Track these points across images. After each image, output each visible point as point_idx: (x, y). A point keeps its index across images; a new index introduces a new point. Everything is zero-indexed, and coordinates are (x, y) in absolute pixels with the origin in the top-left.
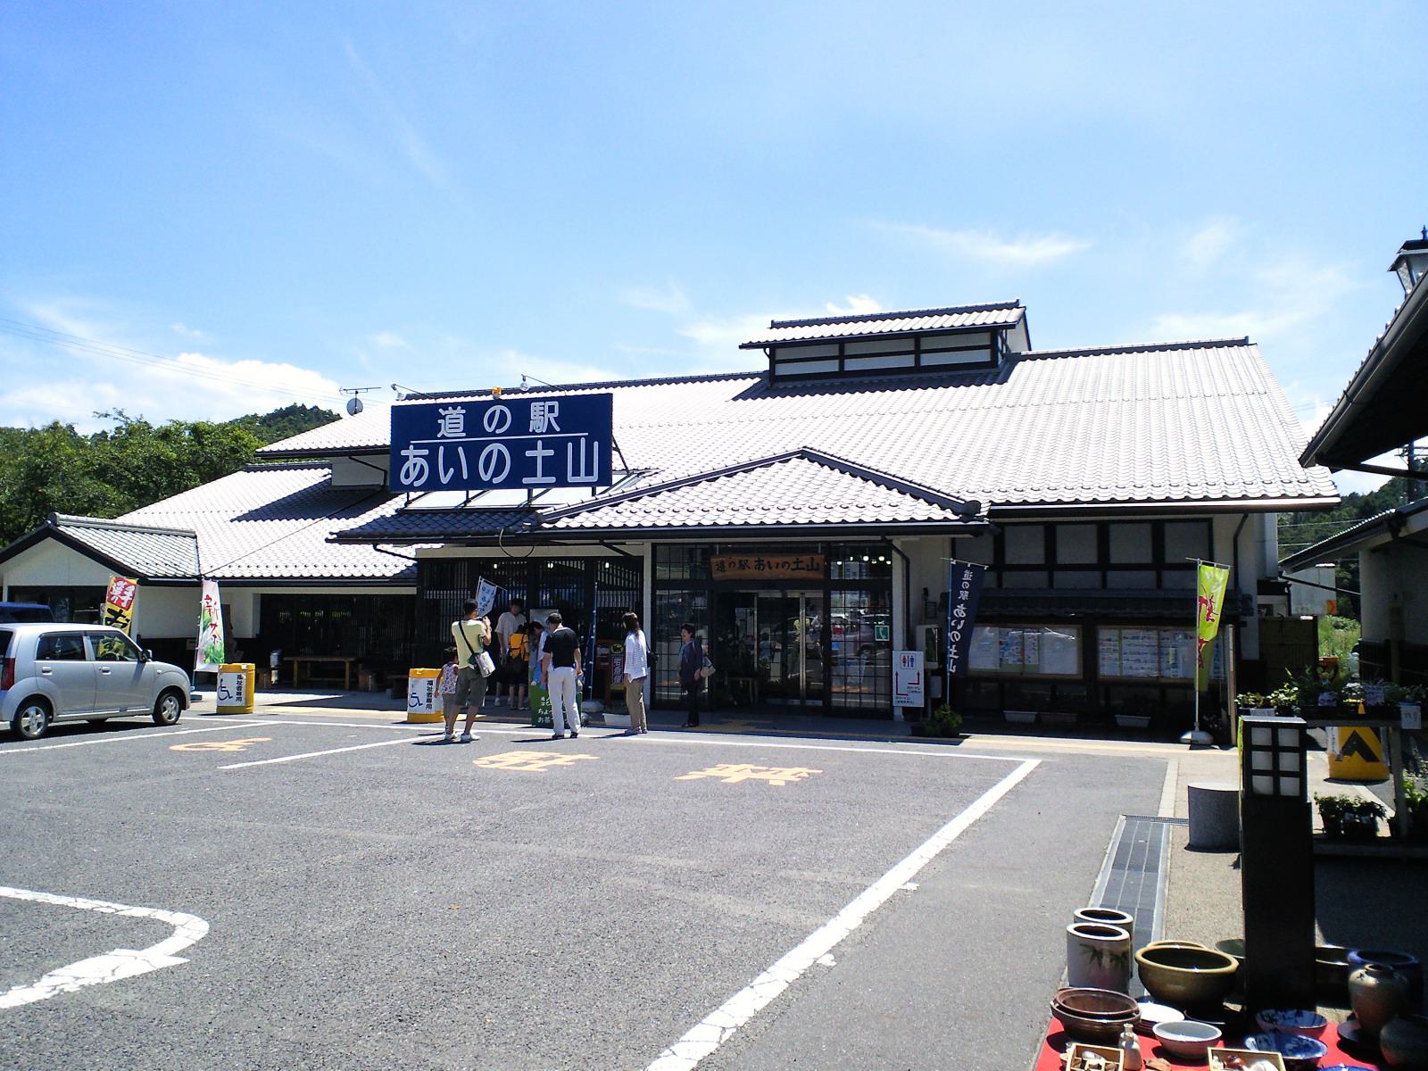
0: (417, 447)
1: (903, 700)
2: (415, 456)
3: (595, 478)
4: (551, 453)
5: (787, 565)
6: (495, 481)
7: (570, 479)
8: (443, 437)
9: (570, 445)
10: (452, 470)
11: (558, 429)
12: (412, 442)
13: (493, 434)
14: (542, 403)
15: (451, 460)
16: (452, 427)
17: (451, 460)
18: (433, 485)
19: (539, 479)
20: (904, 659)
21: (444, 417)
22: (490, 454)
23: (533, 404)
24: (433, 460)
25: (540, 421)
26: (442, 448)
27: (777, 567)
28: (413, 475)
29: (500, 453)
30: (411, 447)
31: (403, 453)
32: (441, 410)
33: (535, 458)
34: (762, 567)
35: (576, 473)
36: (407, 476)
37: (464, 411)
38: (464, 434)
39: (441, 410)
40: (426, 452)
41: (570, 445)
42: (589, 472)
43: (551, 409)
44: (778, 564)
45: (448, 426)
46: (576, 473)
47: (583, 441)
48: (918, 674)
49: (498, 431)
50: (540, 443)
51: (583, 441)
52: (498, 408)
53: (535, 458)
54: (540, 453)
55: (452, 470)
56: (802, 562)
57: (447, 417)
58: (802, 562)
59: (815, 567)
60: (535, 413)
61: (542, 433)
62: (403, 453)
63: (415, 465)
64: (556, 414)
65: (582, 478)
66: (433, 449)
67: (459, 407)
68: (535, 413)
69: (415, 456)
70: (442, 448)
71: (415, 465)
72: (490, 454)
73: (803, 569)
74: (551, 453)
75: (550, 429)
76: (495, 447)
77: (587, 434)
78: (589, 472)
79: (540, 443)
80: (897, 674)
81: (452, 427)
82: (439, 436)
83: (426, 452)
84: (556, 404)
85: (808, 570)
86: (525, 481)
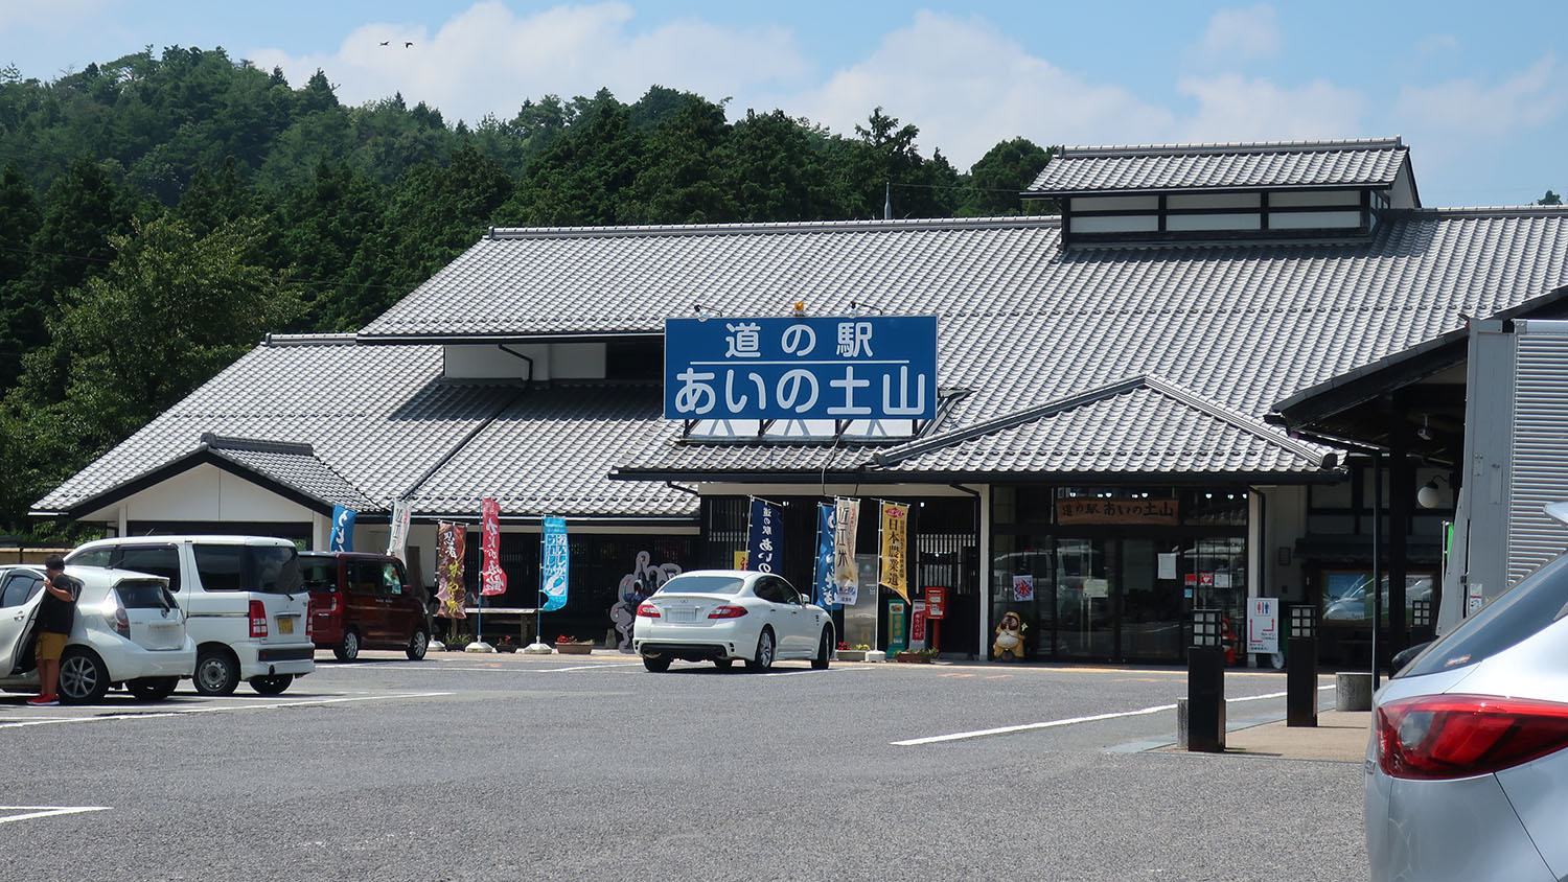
0: (697, 370)
4: (865, 383)
6: (800, 409)
7: (887, 410)
8: (733, 358)
9: (886, 378)
10: (744, 399)
11: (870, 354)
13: (793, 356)
14: (852, 325)
15: (744, 387)
16: (744, 345)
17: (744, 387)
18: (721, 412)
19: (849, 409)
21: (734, 335)
22: (790, 382)
23: (841, 325)
24: (718, 385)
25: (851, 342)
26: (731, 373)
27: (1128, 512)
28: (692, 401)
29: (804, 379)
30: (690, 370)
31: (680, 377)
32: (729, 326)
34: (1112, 511)
35: (895, 402)
36: (684, 402)
38: (758, 354)
39: (729, 326)
40: (711, 376)
41: (886, 378)
43: (864, 331)
46: (895, 402)
47: (904, 370)
49: (799, 353)
50: (850, 370)
51: (904, 370)
52: (799, 328)
54: (849, 383)
55: (744, 399)
56: (1154, 507)
58: (1154, 507)
61: (852, 358)
62: (680, 377)
63: (694, 391)
66: (721, 373)
69: (694, 382)
70: (731, 373)
71: (694, 391)
72: (790, 382)
74: (865, 383)
75: (862, 355)
76: (797, 374)
79: (850, 370)
81: (744, 345)
82: (728, 355)
83: (711, 376)
84: (869, 326)
86: (831, 411)
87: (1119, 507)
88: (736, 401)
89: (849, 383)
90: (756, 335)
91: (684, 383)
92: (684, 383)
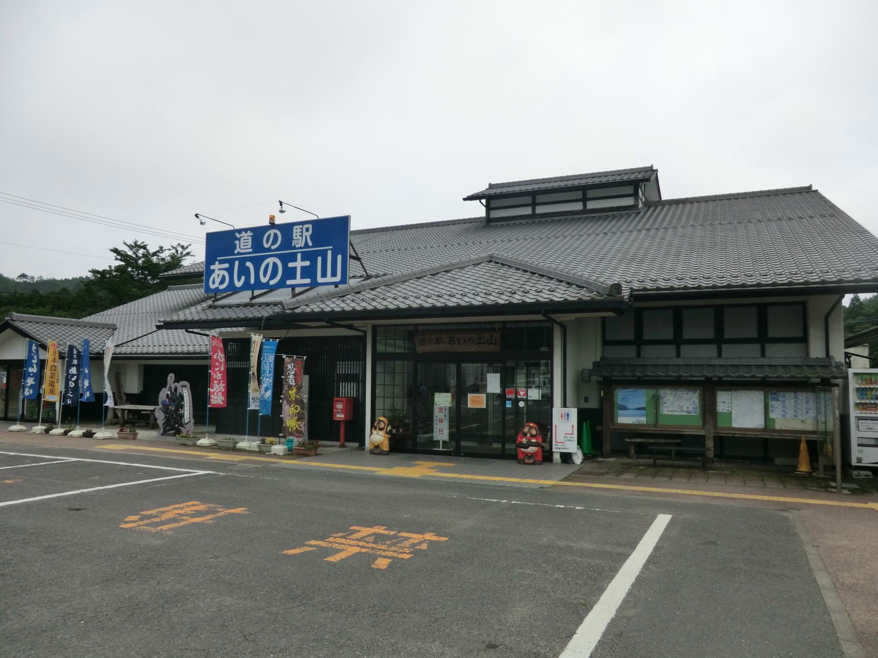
0: (221, 262)
1: (560, 447)
2: (219, 269)
3: (338, 279)
4: (307, 263)
5: (472, 340)
7: (320, 280)
8: (239, 253)
10: (243, 278)
12: (218, 258)
13: (269, 250)
14: (301, 226)
15: (243, 271)
16: (244, 245)
17: (243, 271)
20: (562, 414)
21: (239, 239)
24: (230, 271)
25: (300, 239)
26: (237, 263)
28: (218, 281)
29: (275, 265)
30: (217, 263)
33: (295, 268)
35: (324, 275)
36: (214, 283)
37: (252, 234)
40: (227, 265)
42: (334, 274)
43: (307, 230)
44: (465, 340)
45: (242, 244)
46: (324, 275)
47: (330, 253)
48: (573, 426)
50: (299, 255)
51: (330, 253)
52: (272, 232)
53: (295, 268)
55: (243, 278)
56: (483, 338)
57: (242, 239)
58: (483, 338)
59: (493, 341)
60: (296, 234)
61: (301, 248)
63: (219, 275)
64: (310, 232)
65: (329, 279)
66: (231, 262)
67: (249, 232)
68: (296, 234)
69: (219, 269)
70: (237, 263)
71: (219, 275)
73: (484, 343)
74: (307, 263)
76: (271, 261)
77: (331, 247)
78: (334, 274)
79: (299, 255)
80: (556, 427)
81: (244, 245)
82: (236, 252)
84: (310, 226)
85: (488, 344)
87: (458, 338)
88: (239, 280)
89: (299, 264)
90: (250, 238)
91: (213, 271)
92: (213, 271)
